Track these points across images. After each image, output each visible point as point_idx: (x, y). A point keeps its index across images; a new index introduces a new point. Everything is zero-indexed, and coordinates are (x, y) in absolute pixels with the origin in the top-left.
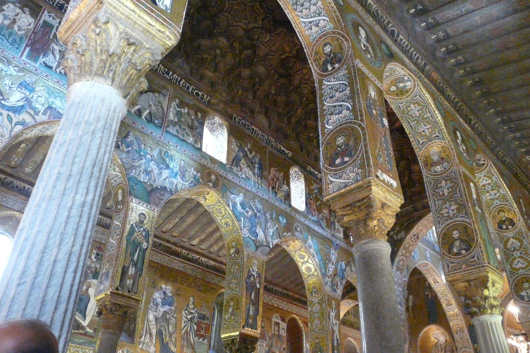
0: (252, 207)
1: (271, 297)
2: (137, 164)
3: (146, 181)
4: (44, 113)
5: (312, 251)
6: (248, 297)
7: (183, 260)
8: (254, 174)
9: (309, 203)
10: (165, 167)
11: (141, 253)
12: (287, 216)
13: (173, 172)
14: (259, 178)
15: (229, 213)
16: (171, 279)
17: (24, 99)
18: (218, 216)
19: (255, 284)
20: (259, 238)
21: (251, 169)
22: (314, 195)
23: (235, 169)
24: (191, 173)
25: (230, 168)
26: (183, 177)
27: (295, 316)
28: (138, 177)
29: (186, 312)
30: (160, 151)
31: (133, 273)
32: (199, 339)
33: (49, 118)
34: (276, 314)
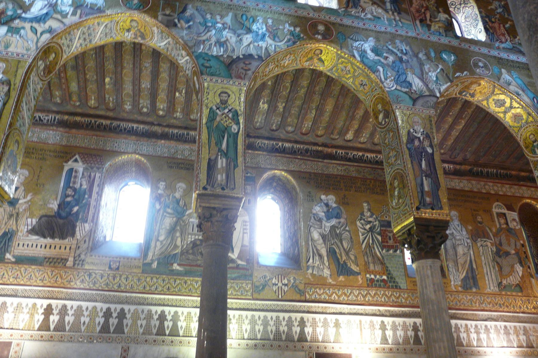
0: (392, 51)
1: (482, 183)
2: (204, 38)
3: (222, 53)
4: (74, 14)
5: (512, 88)
6: (416, 167)
7: (342, 162)
8: (386, 11)
9: (491, 28)
10: (245, 32)
11: (231, 140)
12: (453, 50)
13: (257, 34)
14: (396, 14)
15: (358, 67)
16: (331, 188)
17: (48, 6)
18: (348, 79)
19: (424, 148)
20: (414, 88)
21: (379, 6)
22: (498, 16)
23: (353, 11)
24: (286, 30)
25: (346, 11)
26: (274, 36)
27: (528, 201)
28: (209, 52)
29: (362, 221)
30: (235, 16)
31: (224, 165)
32: (388, 251)
33: (80, 17)
34: (496, 203)
